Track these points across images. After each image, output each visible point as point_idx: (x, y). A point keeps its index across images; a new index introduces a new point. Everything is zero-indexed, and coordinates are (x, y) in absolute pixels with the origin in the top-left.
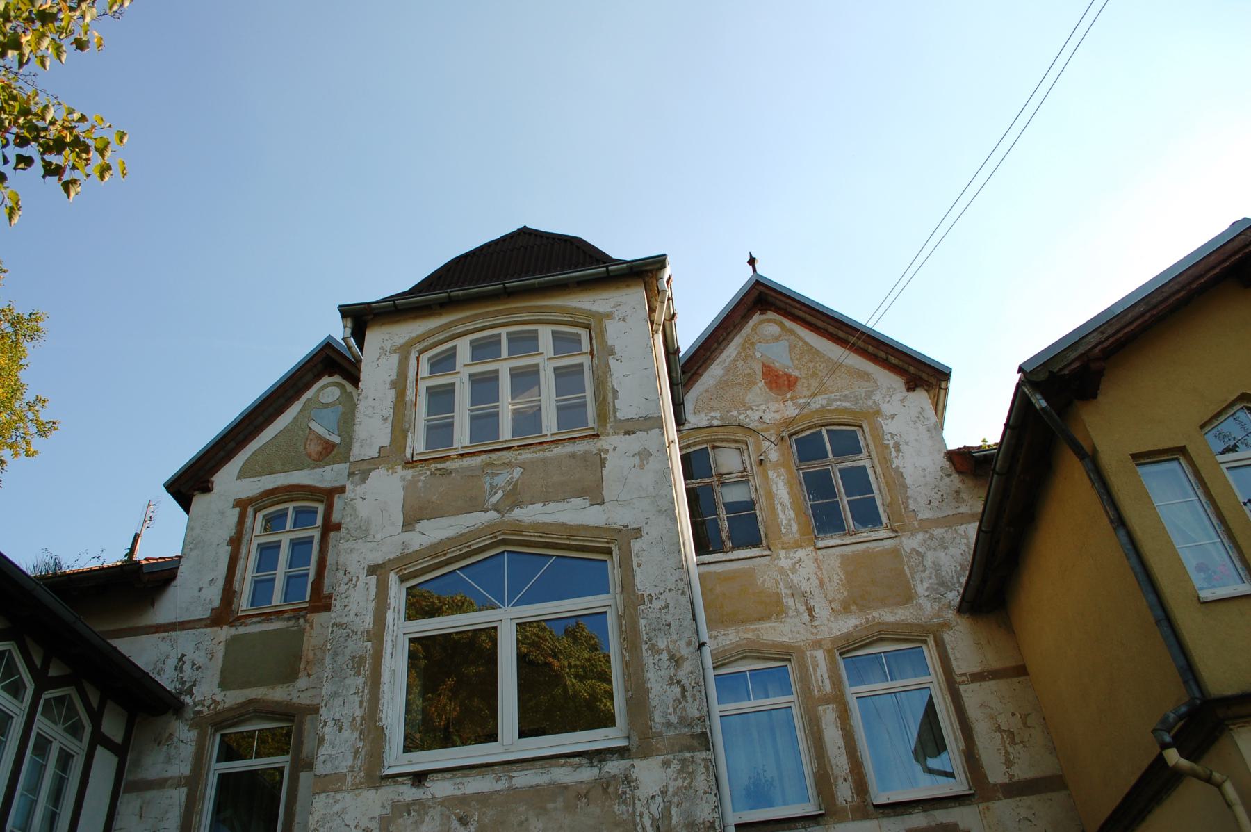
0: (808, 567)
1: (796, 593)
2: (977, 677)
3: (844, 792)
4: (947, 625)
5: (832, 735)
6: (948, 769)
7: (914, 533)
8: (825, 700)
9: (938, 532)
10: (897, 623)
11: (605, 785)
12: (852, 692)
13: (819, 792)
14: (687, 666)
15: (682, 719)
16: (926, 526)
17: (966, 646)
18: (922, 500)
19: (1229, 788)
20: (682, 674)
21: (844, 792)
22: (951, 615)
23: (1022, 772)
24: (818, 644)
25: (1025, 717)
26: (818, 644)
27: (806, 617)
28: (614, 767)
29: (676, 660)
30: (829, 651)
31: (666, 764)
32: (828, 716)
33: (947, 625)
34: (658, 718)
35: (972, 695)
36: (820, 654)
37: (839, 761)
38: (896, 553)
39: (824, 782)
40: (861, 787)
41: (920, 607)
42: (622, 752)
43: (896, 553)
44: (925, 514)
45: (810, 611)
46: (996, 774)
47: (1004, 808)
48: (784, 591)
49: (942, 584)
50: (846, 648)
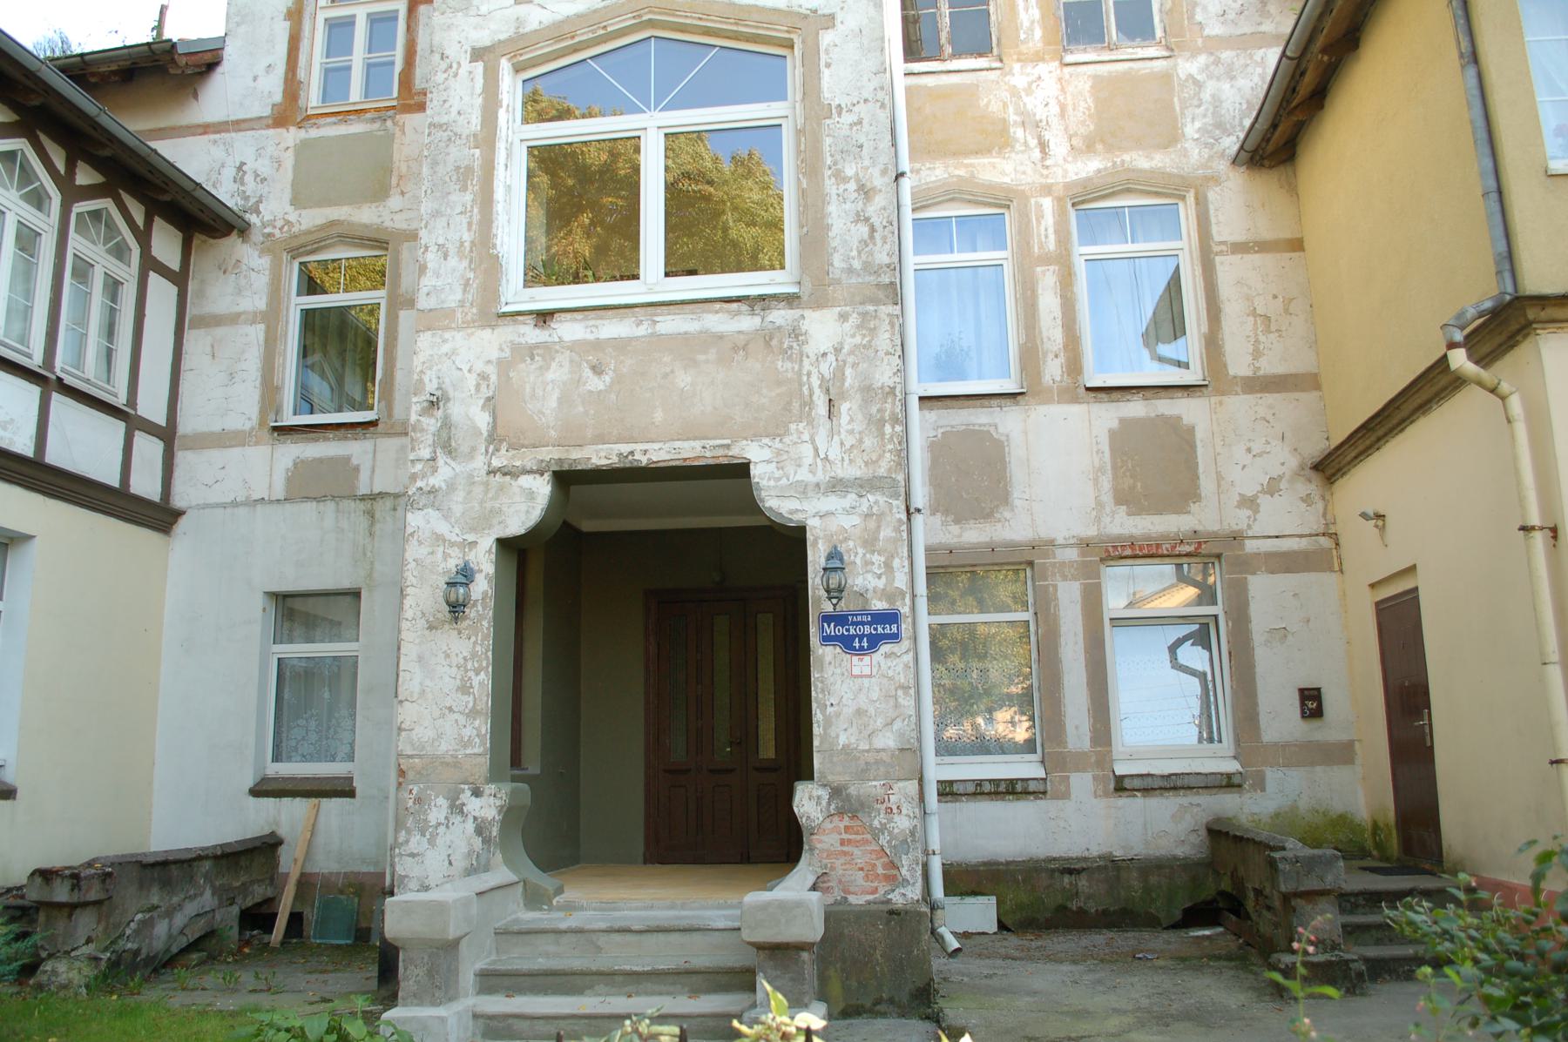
0: (1049, 88)
1: (1032, 123)
2: (1239, 248)
3: (1053, 370)
4: (1215, 180)
5: (1049, 303)
6: (1183, 359)
7: (1194, 54)
8: (1046, 260)
9: (1226, 55)
10: (1152, 171)
11: (767, 337)
12: (1081, 252)
13: (1023, 369)
14: (879, 201)
15: (867, 266)
16: (1213, 45)
17: (1236, 204)
18: (1214, 9)
19: (1515, 403)
20: (871, 210)
21: (1053, 370)
22: (1223, 166)
23: (1271, 365)
24: (1047, 190)
25: (1288, 302)
26: (1047, 190)
27: (1037, 154)
28: (780, 316)
29: (866, 192)
30: (1059, 200)
31: (843, 317)
32: (1047, 280)
33: (1215, 180)
34: (838, 262)
35: (1229, 269)
36: (1047, 203)
37: (1052, 333)
38: (1166, 78)
39: (1030, 357)
40: (1074, 366)
41: (1185, 153)
42: (790, 300)
43: (1166, 78)
44: (1215, 29)
45: (1043, 146)
46: (1239, 363)
47: (1240, 405)
48: (1013, 117)
49: (1218, 125)
50: (1081, 198)
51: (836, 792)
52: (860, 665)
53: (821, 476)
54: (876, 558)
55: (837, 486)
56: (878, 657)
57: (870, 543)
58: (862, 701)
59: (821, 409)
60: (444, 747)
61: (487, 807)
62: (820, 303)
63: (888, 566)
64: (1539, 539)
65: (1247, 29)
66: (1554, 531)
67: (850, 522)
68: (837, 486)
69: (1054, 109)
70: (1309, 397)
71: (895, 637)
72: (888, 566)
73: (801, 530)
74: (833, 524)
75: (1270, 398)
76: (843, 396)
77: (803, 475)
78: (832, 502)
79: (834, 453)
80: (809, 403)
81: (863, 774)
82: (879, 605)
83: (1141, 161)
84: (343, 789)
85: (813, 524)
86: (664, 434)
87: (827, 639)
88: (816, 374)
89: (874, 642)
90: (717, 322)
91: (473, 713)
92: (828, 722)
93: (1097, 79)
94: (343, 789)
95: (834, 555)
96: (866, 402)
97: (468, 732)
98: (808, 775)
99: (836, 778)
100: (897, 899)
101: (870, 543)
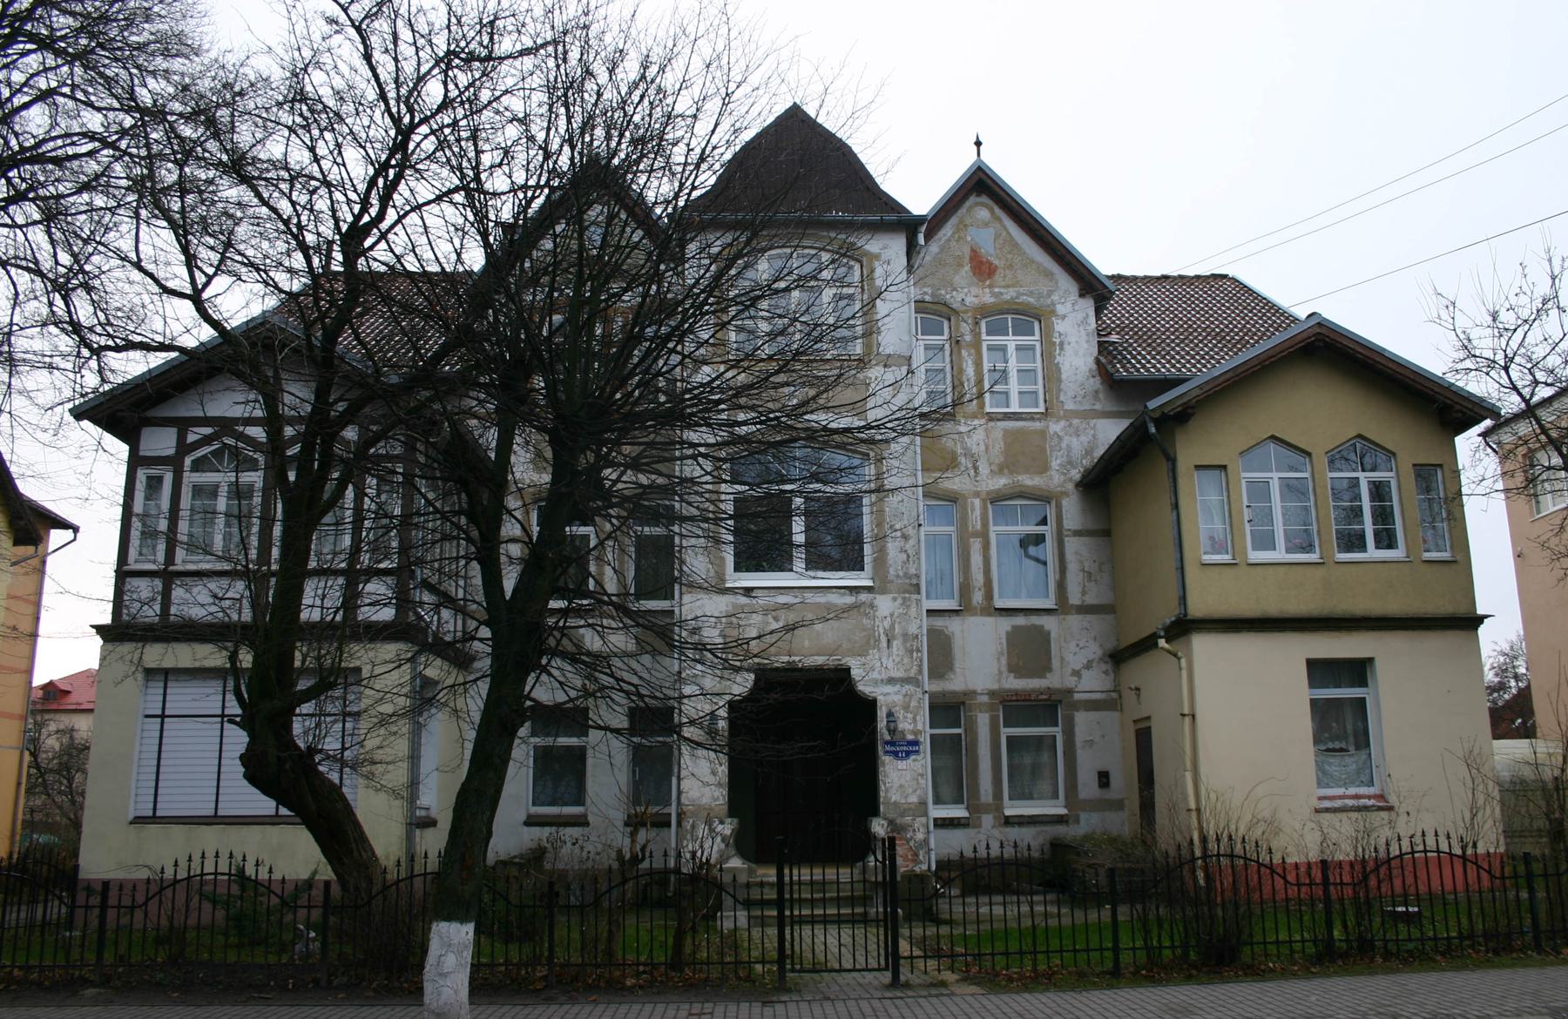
0: (979, 435)
1: (968, 453)
2: (1077, 533)
3: (978, 597)
4: (1066, 494)
5: (976, 559)
6: (1042, 557)
7: (1059, 419)
8: (976, 535)
9: (1076, 422)
10: (1034, 487)
11: (855, 607)
12: (994, 530)
13: (961, 596)
14: (912, 542)
15: (906, 575)
16: (1069, 415)
17: (1072, 512)
18: (1071, 394)
19: (1183, 661)
20: (908, 546)
21: (978, 597)
22: (1070, 487)
23: (1091, 599)
24: (977, 494)
25: (1101, 564)
26: (977, 494)
27: (972, 473)
28: (863, 597)
29: (905, 537)
30: (984, 501)
31: (895, 599)
32: (976, 546)
33: (1066, 494)
34: (892, 571)
35: (1072, 545)
36: (977, 502)
37: (978, 577)
38: (1043, 433)
39: (965, 590)
40: (989, 595)
41: (1051, 478)
42: (869, 589)
43: (1043, 433)
44: (1070, 406)
45: (976, 468)
46: (1074, 598)
47: (1074, 621)
48: (959, 451)
49: (1070, 463)
50: (996, 498)
51: (891, 822)
52: (902, 764)
53: (884, 676)
54: (910, 716)
55: (891, 681)
56: (910, 761)
57: (906, 708)
58: (902, 781)
59: (884, 644)
60: (704, 801)
61: (727, 828)
62: (883, 592)
63: (914, 719)
64: (1187, 719)
65: (1088, 407)
66: (1193, 716)
67: (898, 698)
68: (891, 681)
69: (982, 447)
70: (1109, 617)
71: (917, 752)
72: (914, 719)
73: (875, 701)
74: (890, 699)
75: (1089, 617)
76: (894, 638)
77: (875, 675)
78: (889, 689)
79: (890, 665)
80: (878, 640)
81: (903, 814)
82: (910, 737)
83: (1029, 481)
84: (581, 822)
85: (880, 698)
86: (811, 650)
87: (887, 752)
88: (882, 626)
89: (908, 754)
90: (834, 598)
91: (719, 785)
92: (887, 791)
93: (1006, 432)
94: (581, 822)
95: (890, 714)
96: (905, 641)
97: (717, 794)
98: (876, 813)
99: (891, 816)
100: (917, 869)
101: (906, 708)
